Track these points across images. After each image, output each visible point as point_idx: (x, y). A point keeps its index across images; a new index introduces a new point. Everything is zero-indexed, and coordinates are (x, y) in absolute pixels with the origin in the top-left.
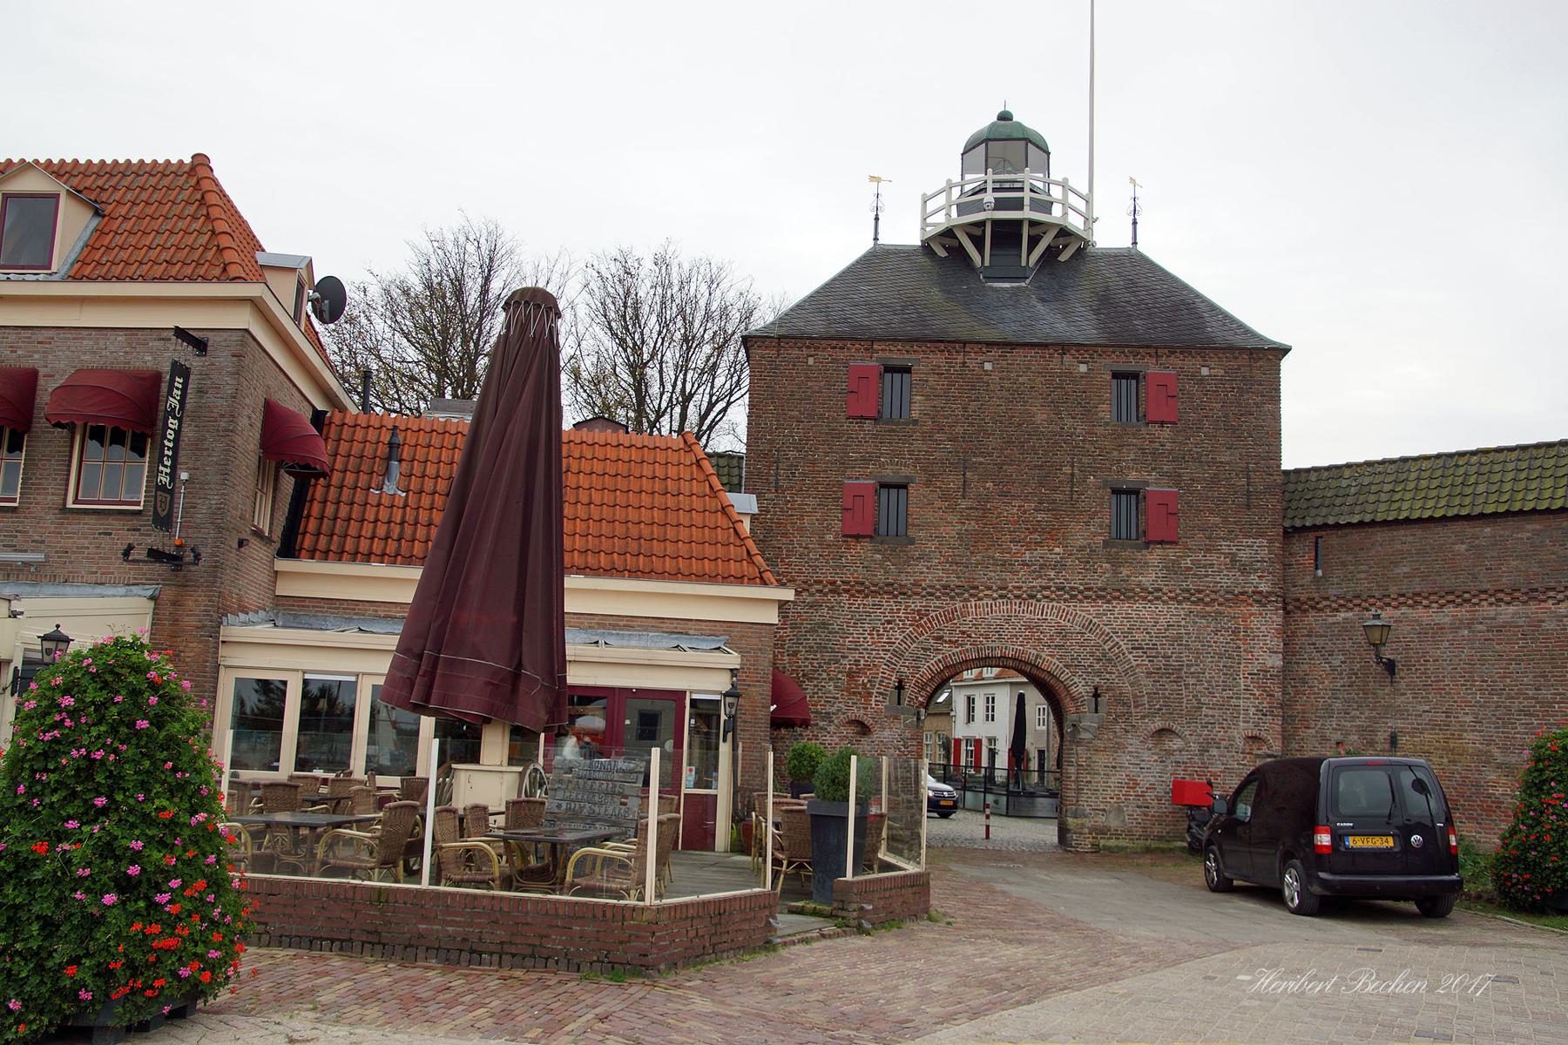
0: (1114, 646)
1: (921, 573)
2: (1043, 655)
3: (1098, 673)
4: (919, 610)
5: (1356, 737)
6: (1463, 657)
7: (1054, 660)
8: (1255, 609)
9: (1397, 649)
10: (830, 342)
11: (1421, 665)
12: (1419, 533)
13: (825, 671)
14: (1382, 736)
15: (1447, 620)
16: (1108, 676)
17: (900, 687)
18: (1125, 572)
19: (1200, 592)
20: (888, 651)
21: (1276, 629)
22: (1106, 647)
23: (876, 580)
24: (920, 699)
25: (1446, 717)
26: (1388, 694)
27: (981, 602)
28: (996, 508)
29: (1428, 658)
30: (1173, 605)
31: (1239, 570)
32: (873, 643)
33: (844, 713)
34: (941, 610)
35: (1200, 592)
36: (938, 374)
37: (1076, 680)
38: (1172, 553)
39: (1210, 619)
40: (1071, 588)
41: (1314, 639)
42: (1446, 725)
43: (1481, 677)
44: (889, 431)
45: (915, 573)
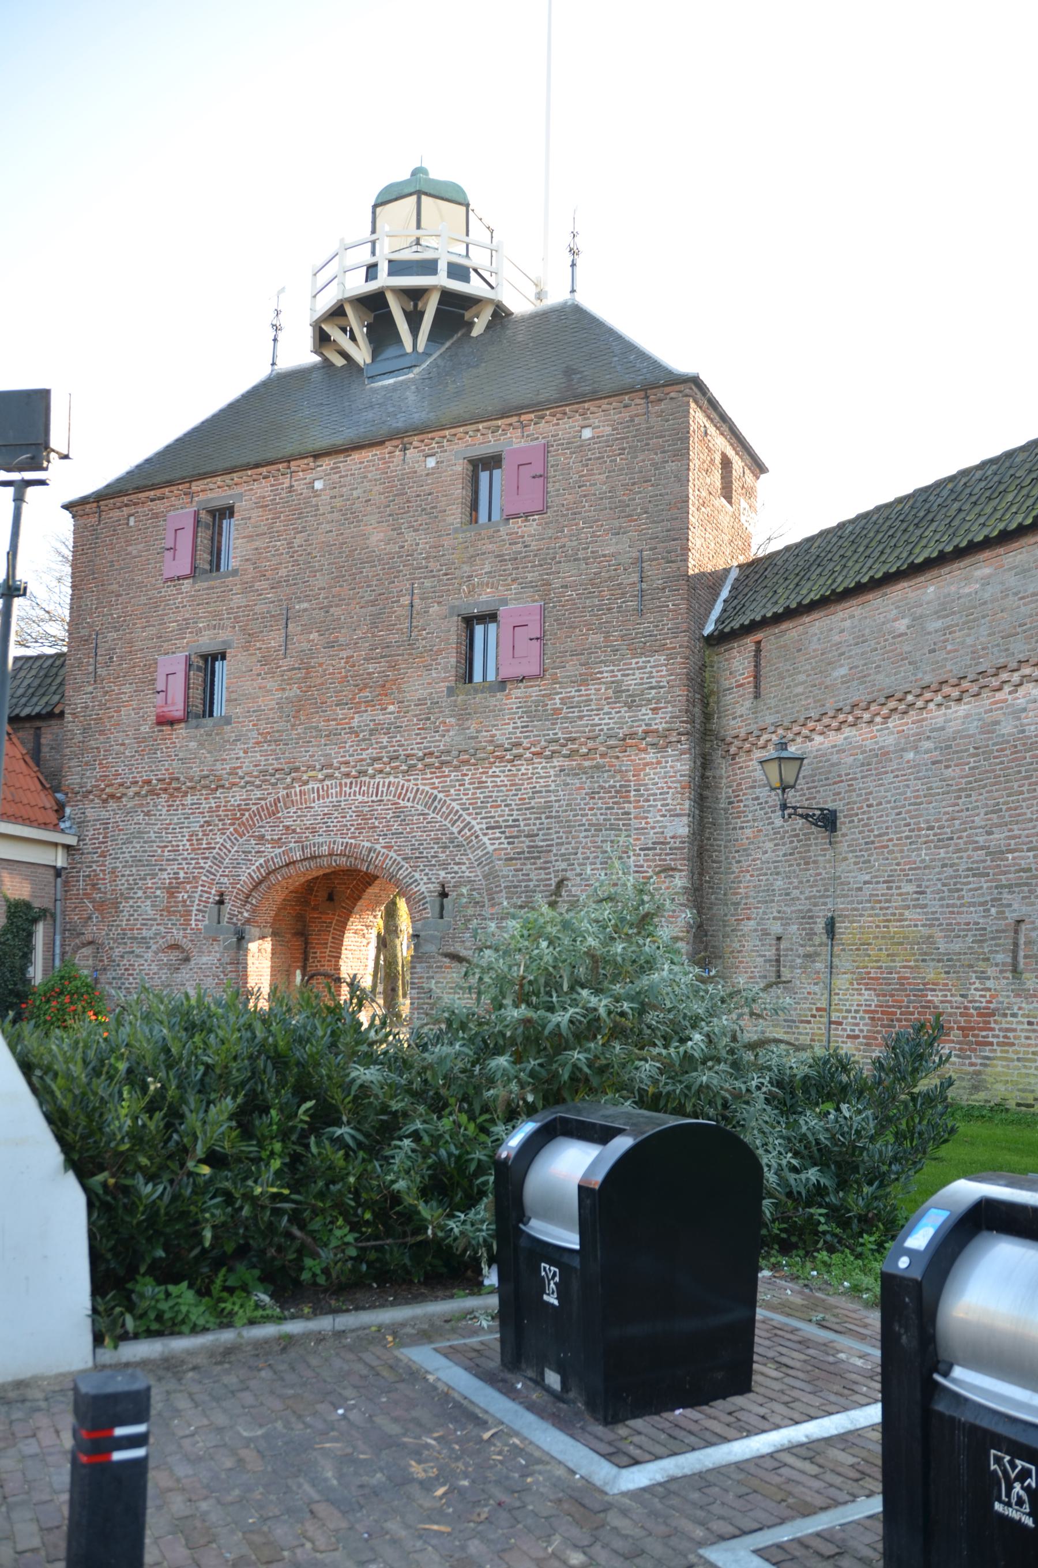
0: (465, 827)
1: (237, 759)
2: (378, 847)
3: (444, 865)
4: (239, 805)
5: (796, 927)
6: (909, 794)
7: (392, 854)
8: (650, 756)
9: (839, 793)
10: (147, 494)
11: (864, 813)
12: (857, 611)
13: (140, 888)
14: (820, 926)
15: (890, 740)
16: (456, 868)
17: (221, 902)
18: (473, 726)
19: (573, 740)
20: (207, 858)
21: (680, 782)
22: (455, 830)
23: (191, 773)
24: (246, 914)
25: (889, 888)
26: (829, 861)
27: (306, 787)
28: (321, 665)
29: (871, 801)
30: (540, 763)
31: (626, 704)
32: (193, 850)
33: (164, 937)
34: (263, 802)
35: (573, 740)
36: (262, 507)
37: (417, 875)
38: (534, 691)
39: (584, 776)
40: (408, 756)
41: (758, 790)
42: (887, 901)
43: (927, 821)
44: (208, 589)
45: (231, 759)
